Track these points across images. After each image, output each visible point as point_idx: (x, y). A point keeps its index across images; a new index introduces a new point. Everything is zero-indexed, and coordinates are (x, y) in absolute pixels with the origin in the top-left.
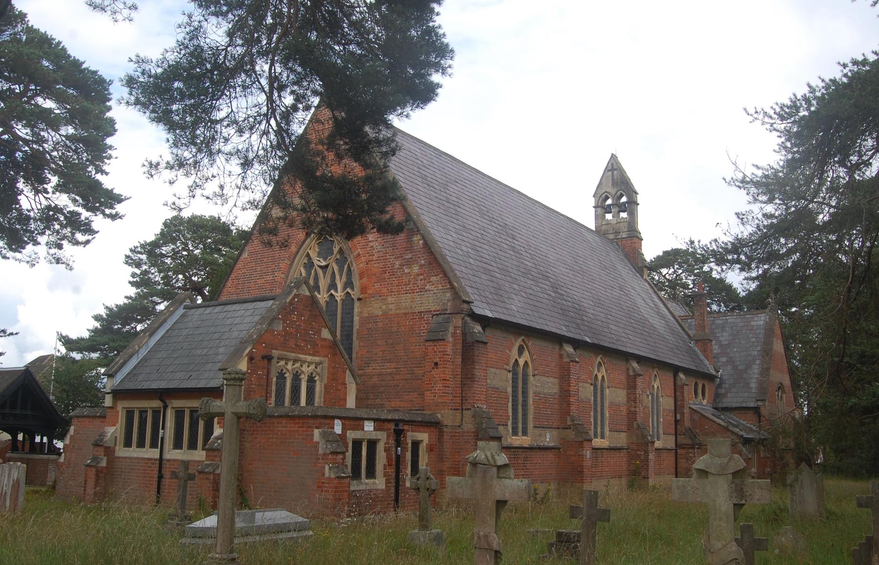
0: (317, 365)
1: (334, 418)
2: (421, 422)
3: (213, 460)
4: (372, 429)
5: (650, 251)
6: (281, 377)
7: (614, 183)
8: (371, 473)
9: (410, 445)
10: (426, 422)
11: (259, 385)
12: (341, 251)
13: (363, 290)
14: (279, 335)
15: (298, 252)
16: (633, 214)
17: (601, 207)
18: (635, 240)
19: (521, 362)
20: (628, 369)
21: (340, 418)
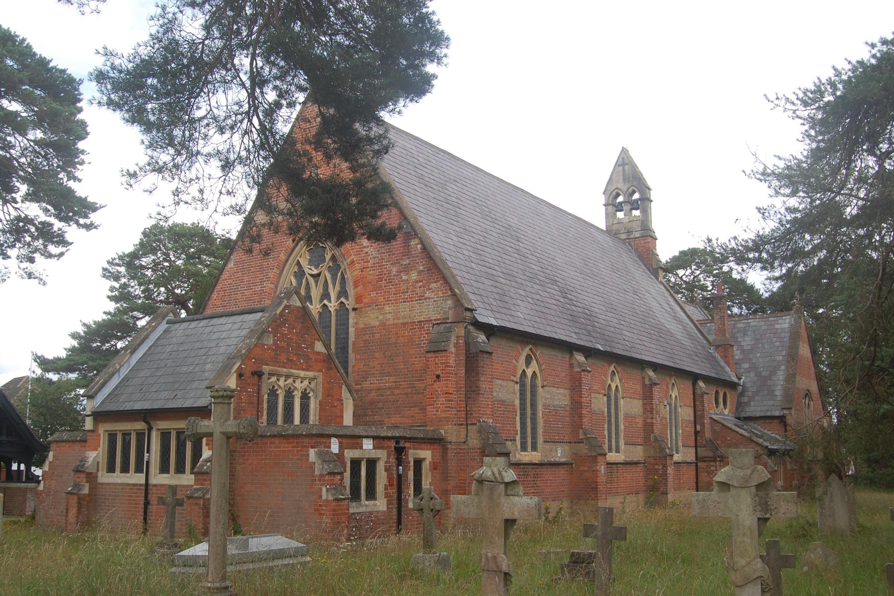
0: (311, 380)
1: (330, 436)
2: (423, 439)
3: (202, 484)
4: (371, 447)
5: (665, 252)
6: (273, 393)
8: (371, 494)
9: (412, 464)
10: (429, 439)
11: (251, 403)
12: (333, 258)
13: (358, 299)
14: (269, 349)
15: (287, 261)
16: (646, 212)
17: (613, 205)
18: (649, 240)
19: (529, 373)
20: (643, 378)
21: (336, 436)
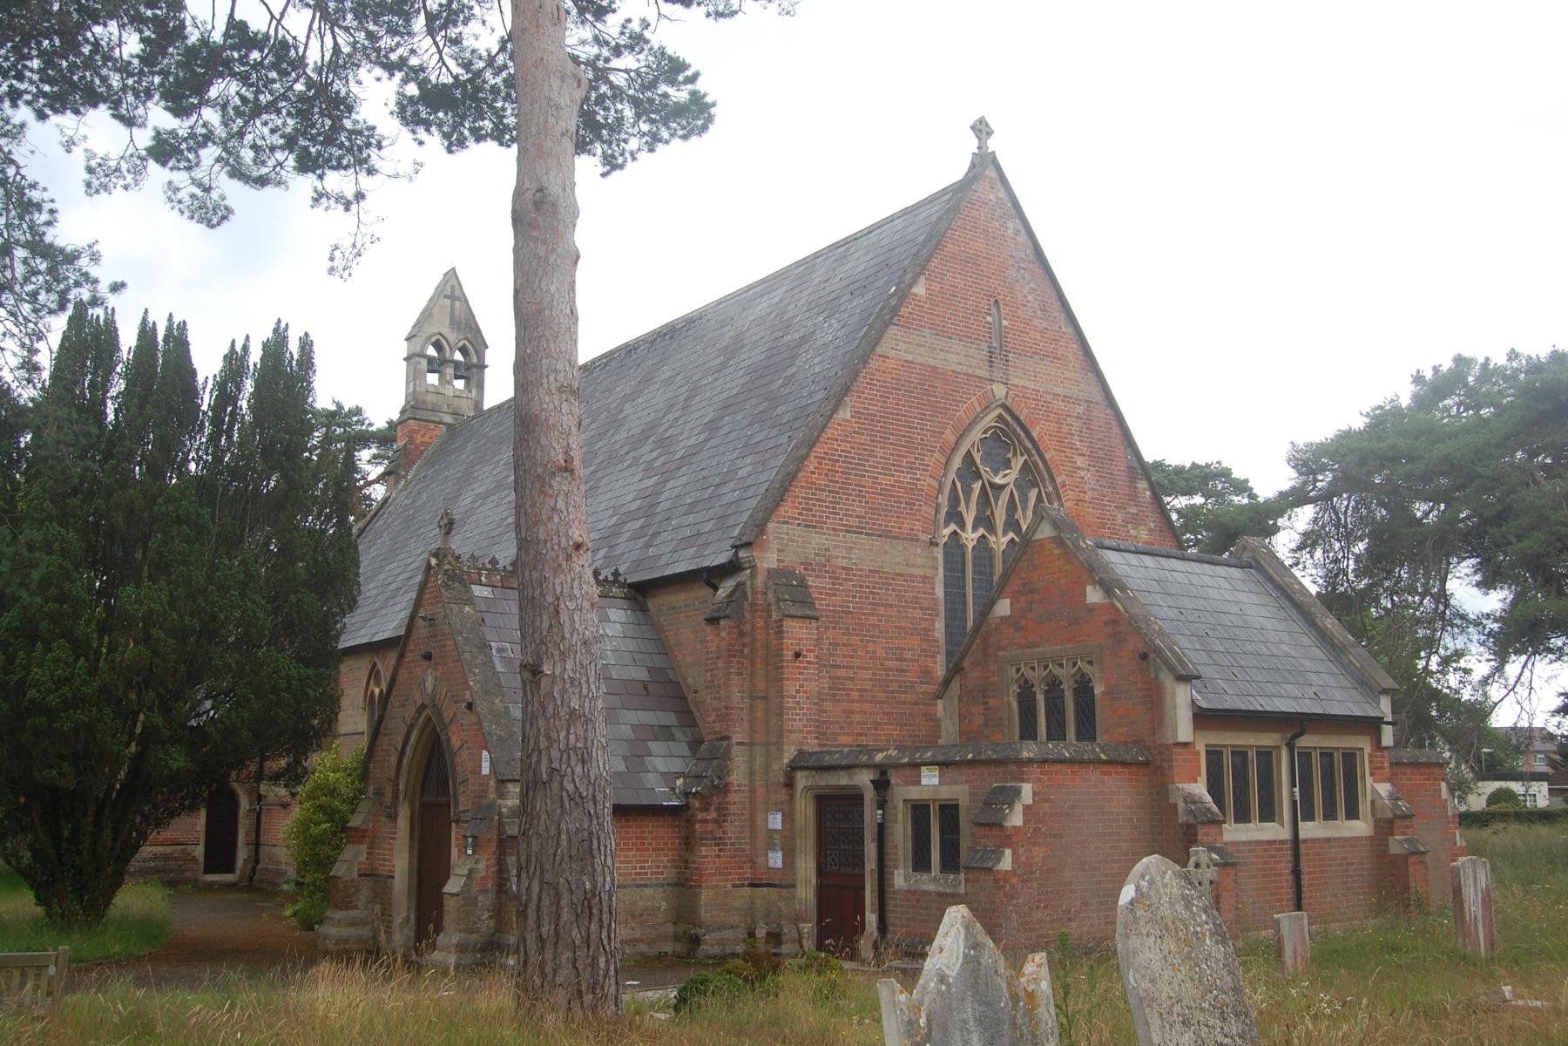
4: (936, 781)
7: (454, 324)
